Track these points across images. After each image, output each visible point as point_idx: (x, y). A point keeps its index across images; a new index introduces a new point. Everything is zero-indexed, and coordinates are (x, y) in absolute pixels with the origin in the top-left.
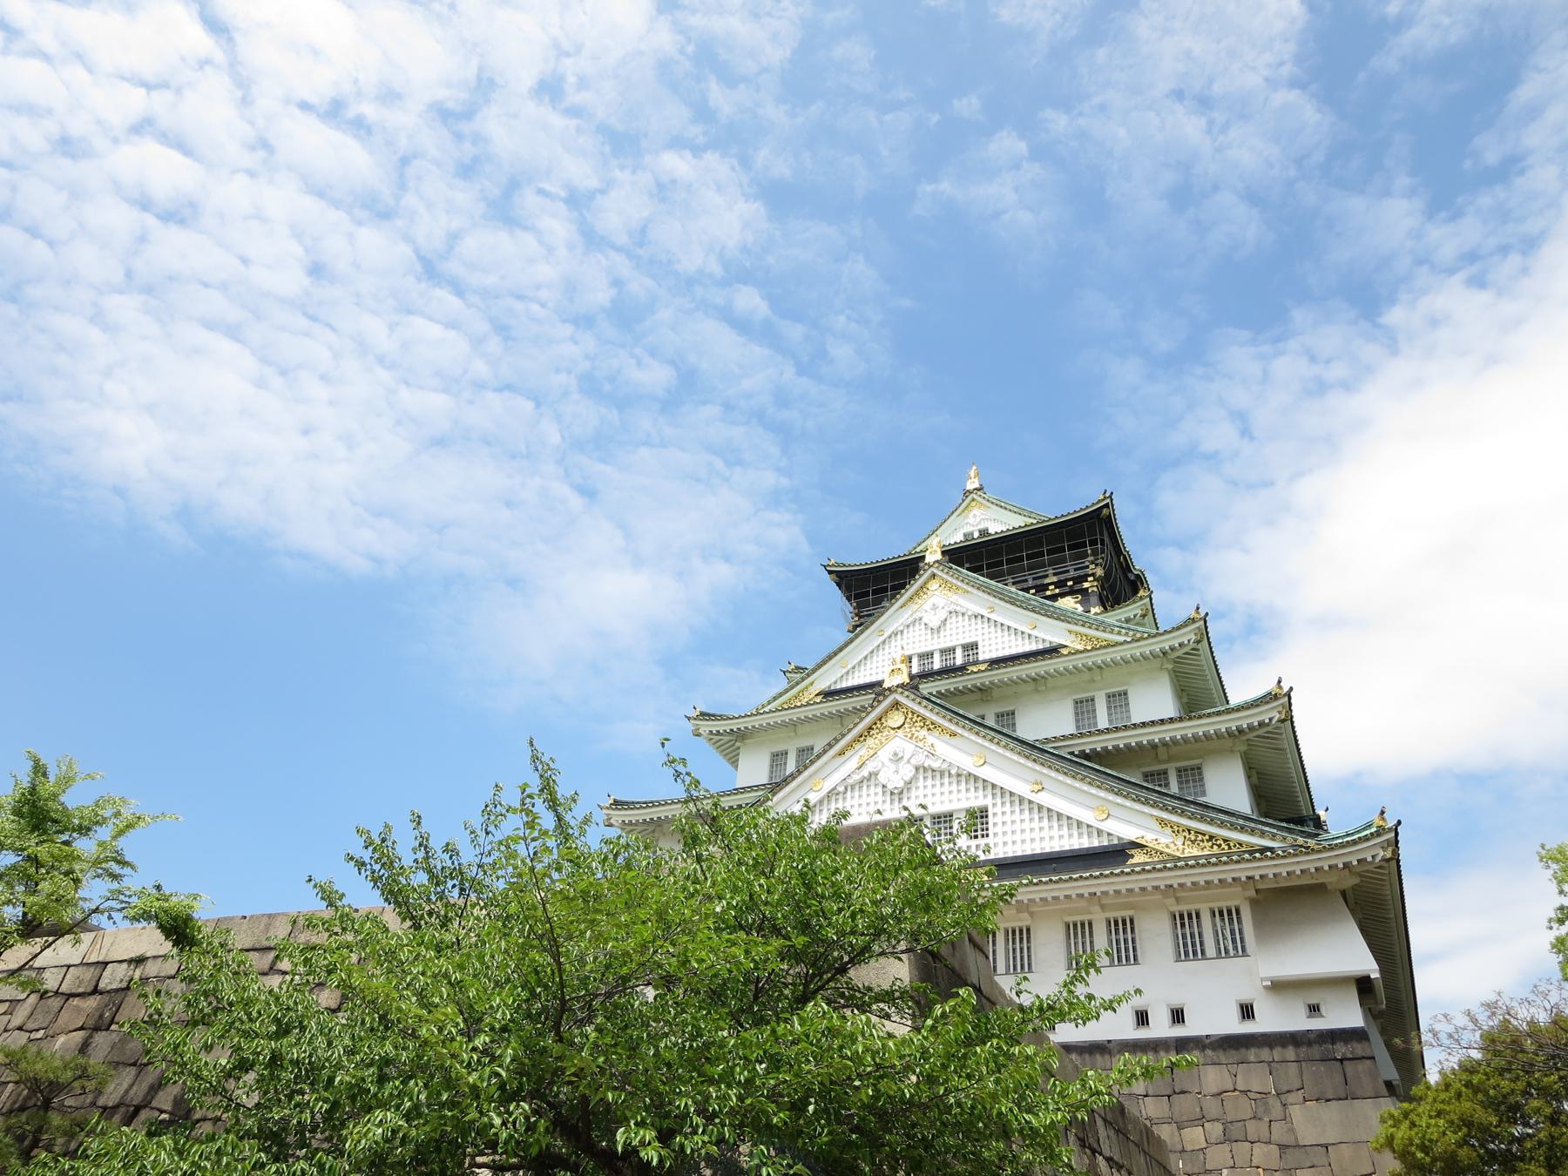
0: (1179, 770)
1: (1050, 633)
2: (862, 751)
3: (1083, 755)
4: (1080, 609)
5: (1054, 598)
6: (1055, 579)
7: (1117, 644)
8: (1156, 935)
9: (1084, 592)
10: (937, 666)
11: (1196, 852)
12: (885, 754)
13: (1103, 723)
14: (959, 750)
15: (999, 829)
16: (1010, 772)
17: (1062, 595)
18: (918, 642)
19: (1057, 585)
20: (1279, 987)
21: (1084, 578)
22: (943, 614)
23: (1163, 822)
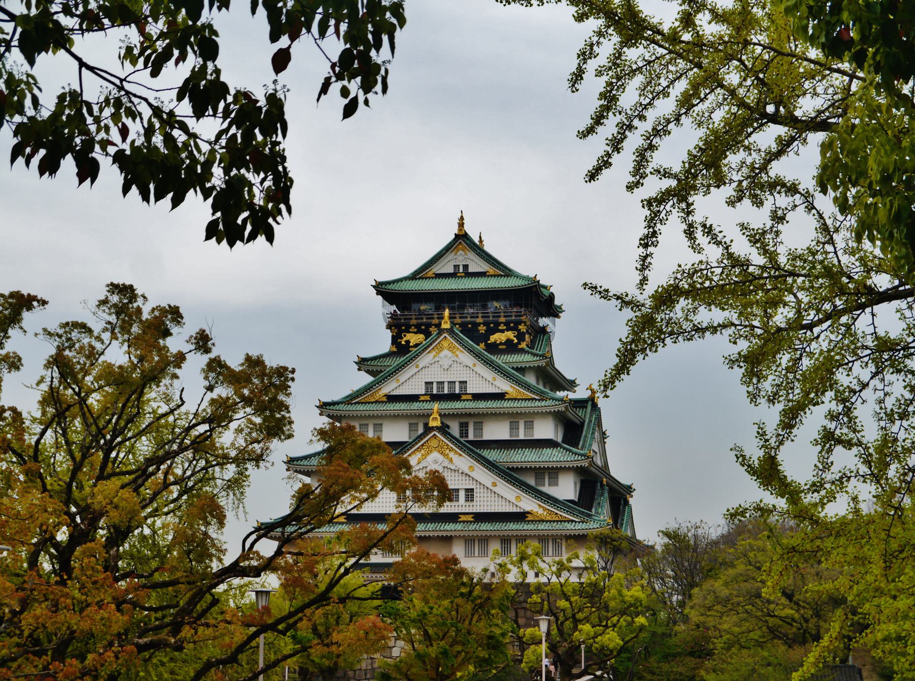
0: (549, 474)
1: (503, 385)
3: (512, 469)
4: (516, 341)
5: (503, 331)
7: (533, 399)
9: (519, 331)
10: (446, 392)
11: (550, 519)
13: (522, 436)
14: (463, 462)
15: (478, 499)
16: (484, 476)
18: (435, 375)
19: (507, 324)
21: (520, 323)
22: (450, 362)
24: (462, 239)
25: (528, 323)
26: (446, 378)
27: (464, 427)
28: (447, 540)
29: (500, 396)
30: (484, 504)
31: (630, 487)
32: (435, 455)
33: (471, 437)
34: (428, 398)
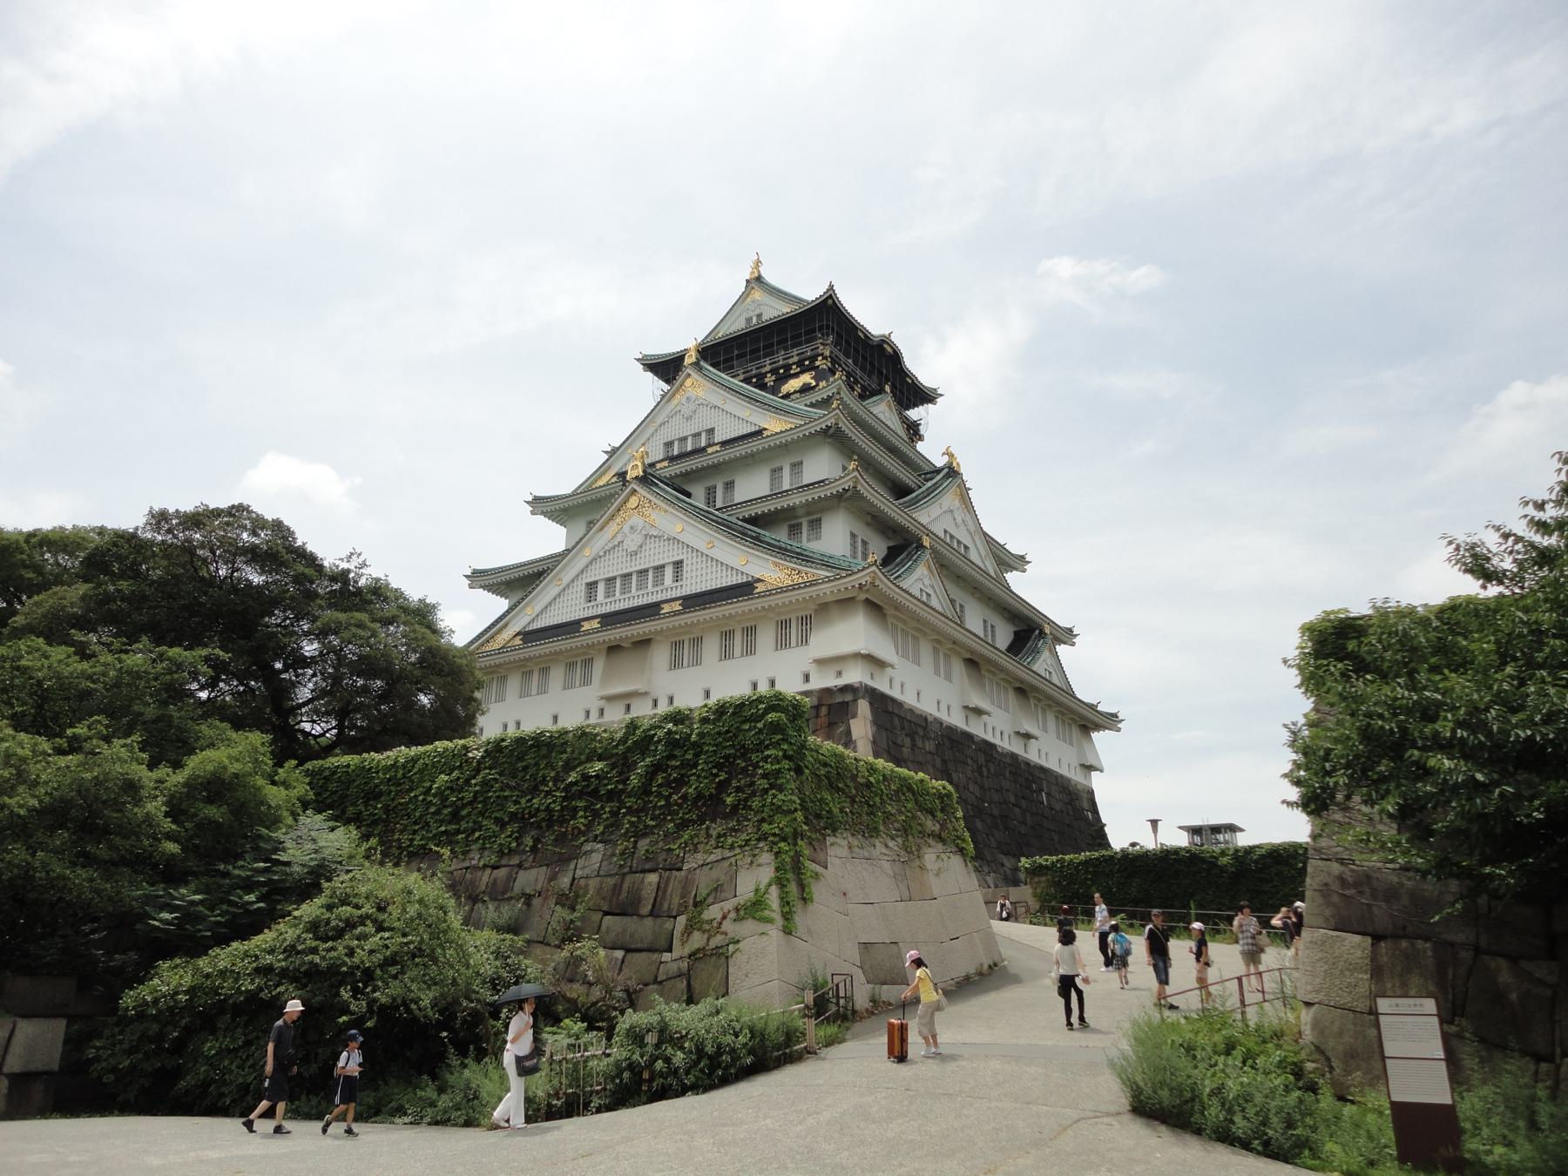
2: (613, 528)
3: (744, 520)
5: (796, 375)
6: (795, 359)
8: (766, 637)
10: (689, 449)
12: (626, 528)
13: (786, 486)
16: (698, 536)
17: (802, 372)
19: (800, 363)
20: (821, 662)
23: (776, 565)
24: (757, 281)
25: (827, 353)
26: (688, 429)
27: (711, 493)
28: (644, 643)
29: (759, 433)
30: (698, 580)
31: (1070, 630)
32: (636, 520)
33: (719, 504)
34: (666, 463)
